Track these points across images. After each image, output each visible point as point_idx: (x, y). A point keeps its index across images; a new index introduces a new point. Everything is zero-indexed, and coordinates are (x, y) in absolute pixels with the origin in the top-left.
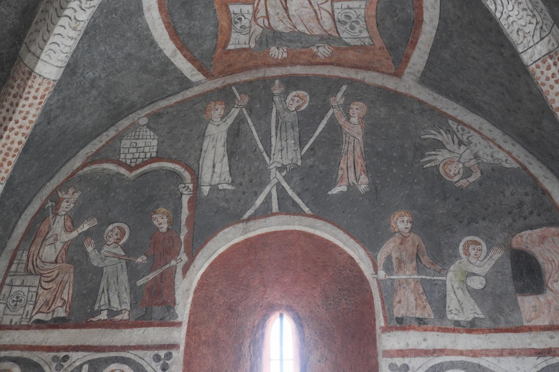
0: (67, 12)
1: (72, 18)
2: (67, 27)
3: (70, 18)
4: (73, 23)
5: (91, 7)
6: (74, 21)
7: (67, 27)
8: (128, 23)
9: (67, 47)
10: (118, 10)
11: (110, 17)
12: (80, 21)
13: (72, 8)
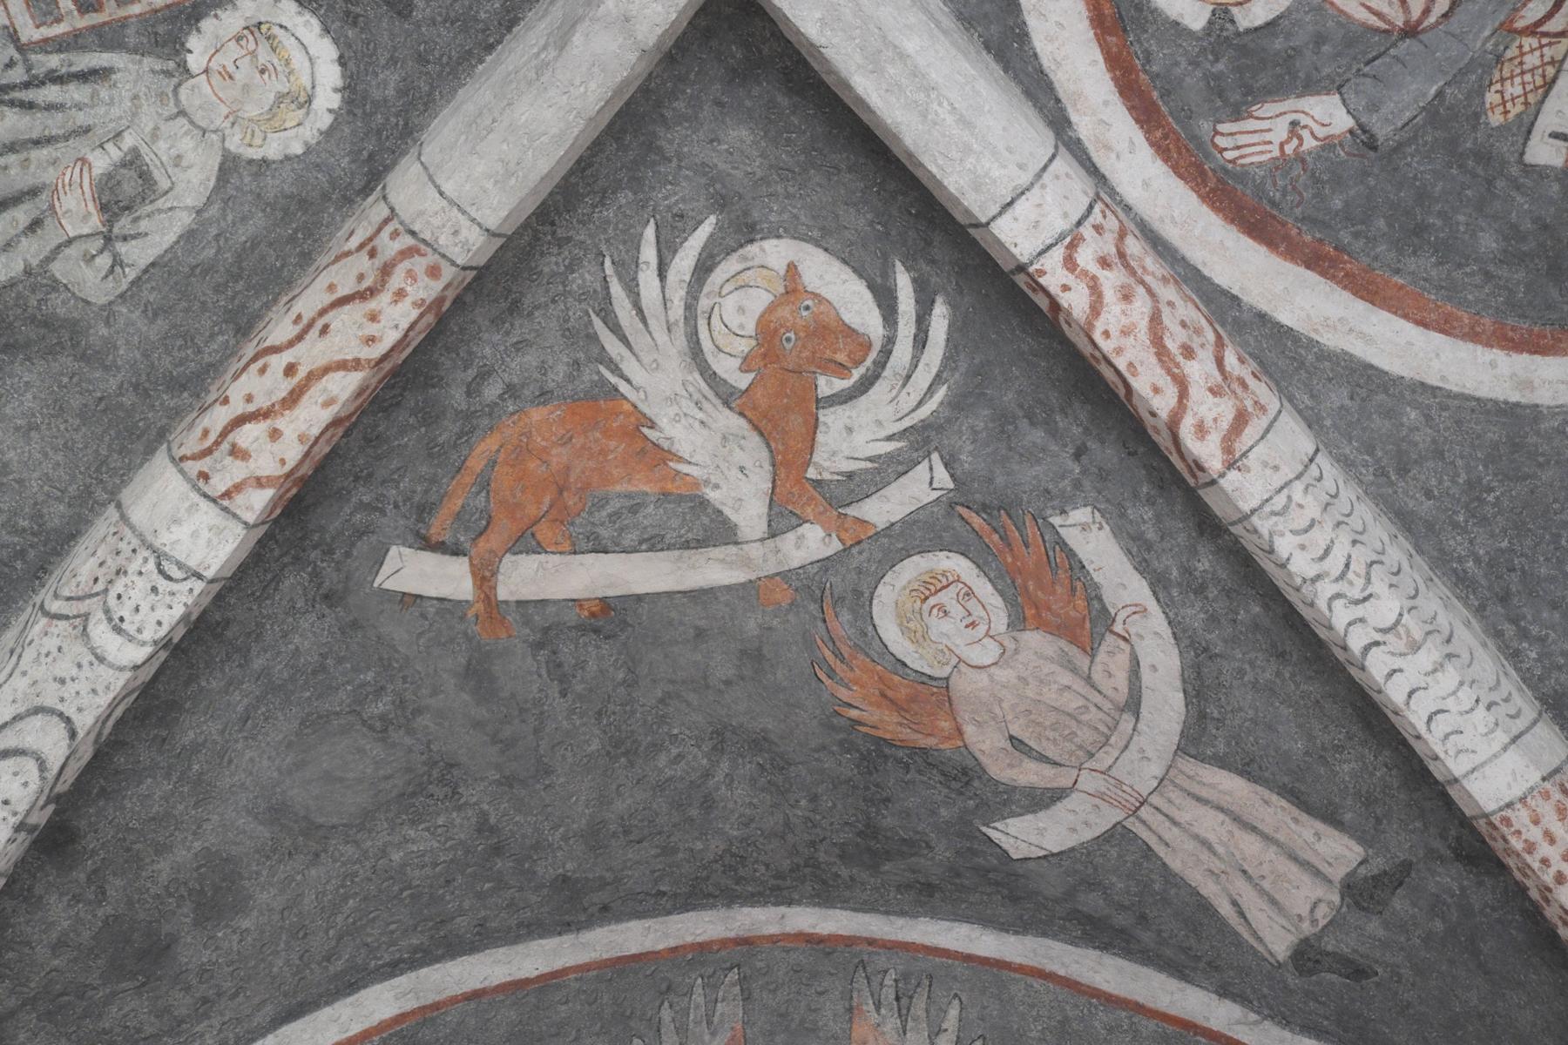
0: (1356, 642)
1: (1378, 637)
2: (1397, 663)
3: (1377, 644)
4: (1395, 643)
5: (1368, 574)
6: (1390, 637)
7: (1397, 663)
8: (1540, 465)
9: (1459, 694)
10: (1480, 479)
11: (1489, 511)
12: (1398, 622)
13: (1350, 624)
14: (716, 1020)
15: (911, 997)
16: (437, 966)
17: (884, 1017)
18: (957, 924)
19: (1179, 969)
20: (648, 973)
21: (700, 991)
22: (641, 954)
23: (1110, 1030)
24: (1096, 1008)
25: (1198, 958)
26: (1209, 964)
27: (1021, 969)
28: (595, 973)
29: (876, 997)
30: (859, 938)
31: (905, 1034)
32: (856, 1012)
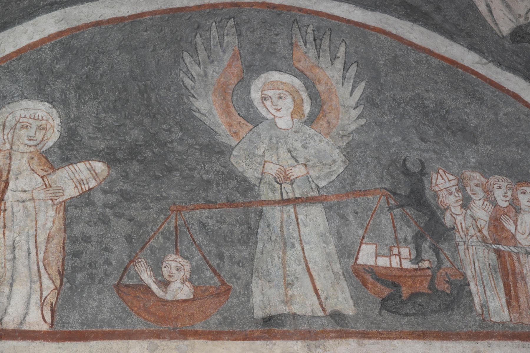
14: (225, 45)
15: (321, 40)
16: (75, 7)
17: (309, 49)
18: (342, 3)
19: (451, 36)
20: (187, 18)
21: (215, 29)
22: (182, 8)
23: (417, 62)
24: (410, 51)
25: (462, 30)
26: (467, 33)
27: (374, 29)
28: (159, 16)
29: (304, 38)
30: (294, 7)
31: (319, 57)
32: (294, 45)
